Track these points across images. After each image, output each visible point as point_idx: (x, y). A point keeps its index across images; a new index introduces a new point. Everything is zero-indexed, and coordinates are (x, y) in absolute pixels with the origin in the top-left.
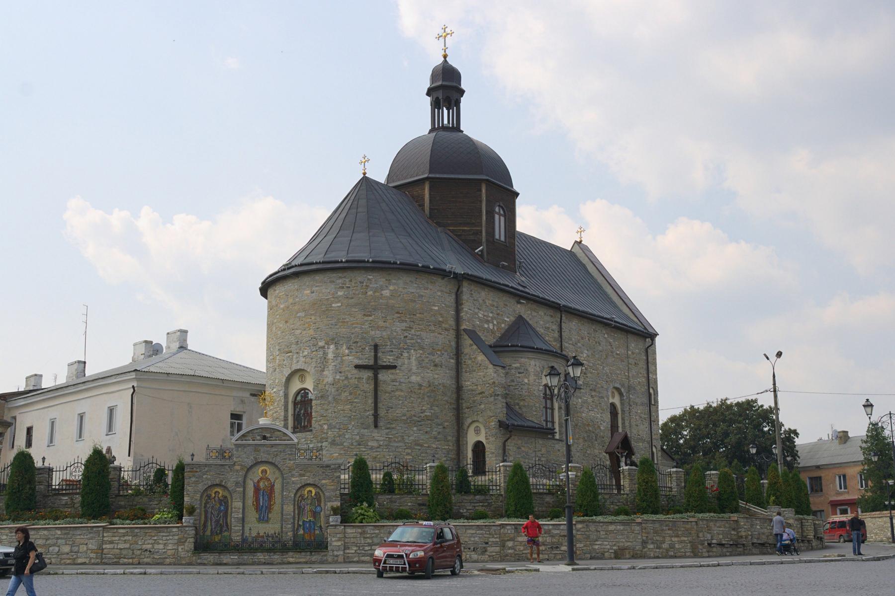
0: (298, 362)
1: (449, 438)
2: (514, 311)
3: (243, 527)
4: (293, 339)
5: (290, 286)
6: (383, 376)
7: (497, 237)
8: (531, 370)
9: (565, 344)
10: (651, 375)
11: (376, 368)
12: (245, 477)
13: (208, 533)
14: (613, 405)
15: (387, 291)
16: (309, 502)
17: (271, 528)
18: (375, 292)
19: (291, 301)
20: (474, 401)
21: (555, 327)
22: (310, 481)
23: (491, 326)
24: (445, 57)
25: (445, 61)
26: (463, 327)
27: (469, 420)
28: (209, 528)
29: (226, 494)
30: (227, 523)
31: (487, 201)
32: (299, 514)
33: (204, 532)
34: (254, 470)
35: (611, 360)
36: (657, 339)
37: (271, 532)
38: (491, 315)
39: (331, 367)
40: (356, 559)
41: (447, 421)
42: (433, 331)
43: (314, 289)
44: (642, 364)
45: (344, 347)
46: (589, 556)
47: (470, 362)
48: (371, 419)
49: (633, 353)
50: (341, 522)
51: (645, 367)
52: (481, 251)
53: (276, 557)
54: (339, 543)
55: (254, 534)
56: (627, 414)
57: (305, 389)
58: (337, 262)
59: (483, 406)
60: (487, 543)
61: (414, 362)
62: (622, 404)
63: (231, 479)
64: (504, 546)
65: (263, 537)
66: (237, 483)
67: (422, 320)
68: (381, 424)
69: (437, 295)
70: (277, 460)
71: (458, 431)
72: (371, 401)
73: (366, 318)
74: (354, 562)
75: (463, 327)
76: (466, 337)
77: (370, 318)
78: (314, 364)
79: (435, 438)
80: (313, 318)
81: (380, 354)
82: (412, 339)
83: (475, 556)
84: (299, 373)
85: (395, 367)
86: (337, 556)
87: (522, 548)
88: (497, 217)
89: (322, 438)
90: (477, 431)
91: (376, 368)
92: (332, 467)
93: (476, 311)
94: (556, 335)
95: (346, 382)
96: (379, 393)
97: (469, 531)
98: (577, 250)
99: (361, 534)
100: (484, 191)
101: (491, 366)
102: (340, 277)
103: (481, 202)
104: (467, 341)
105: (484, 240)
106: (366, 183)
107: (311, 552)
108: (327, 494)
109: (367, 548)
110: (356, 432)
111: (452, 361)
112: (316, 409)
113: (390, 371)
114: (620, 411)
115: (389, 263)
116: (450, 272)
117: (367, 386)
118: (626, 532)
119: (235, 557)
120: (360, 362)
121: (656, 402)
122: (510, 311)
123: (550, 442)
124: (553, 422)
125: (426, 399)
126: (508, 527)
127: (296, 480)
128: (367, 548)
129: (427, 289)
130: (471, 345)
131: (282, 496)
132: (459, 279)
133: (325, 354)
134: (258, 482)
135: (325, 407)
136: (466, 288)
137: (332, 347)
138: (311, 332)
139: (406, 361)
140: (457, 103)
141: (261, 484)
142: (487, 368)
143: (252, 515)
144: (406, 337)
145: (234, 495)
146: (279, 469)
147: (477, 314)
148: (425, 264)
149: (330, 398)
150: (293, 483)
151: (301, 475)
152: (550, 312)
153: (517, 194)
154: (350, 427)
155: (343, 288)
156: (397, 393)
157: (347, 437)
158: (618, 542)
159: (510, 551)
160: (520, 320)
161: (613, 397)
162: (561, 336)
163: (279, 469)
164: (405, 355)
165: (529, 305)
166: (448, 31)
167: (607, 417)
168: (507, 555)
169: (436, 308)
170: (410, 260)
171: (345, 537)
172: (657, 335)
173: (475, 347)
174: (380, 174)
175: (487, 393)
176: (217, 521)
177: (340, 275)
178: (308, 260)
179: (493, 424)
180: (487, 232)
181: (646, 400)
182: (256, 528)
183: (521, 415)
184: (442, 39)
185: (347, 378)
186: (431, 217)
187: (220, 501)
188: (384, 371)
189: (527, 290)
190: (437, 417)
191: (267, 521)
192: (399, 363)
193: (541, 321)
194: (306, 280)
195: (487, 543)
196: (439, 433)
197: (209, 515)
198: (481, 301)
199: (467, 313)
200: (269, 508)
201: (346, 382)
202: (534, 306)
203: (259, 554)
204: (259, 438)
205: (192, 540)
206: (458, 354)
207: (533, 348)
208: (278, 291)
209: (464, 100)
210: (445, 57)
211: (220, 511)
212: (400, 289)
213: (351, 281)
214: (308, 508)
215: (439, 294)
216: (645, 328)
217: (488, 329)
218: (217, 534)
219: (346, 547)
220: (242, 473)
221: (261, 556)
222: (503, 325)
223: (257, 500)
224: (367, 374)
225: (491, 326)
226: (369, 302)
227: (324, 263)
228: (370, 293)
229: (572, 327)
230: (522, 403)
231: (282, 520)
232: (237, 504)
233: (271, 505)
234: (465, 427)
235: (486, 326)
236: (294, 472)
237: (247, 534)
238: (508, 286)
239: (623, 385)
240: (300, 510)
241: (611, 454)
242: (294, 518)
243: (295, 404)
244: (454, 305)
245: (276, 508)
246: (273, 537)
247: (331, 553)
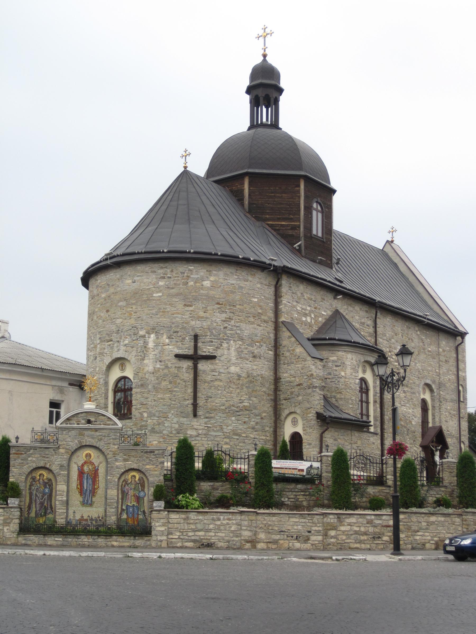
0: (118, 350)
1: (267, 429)
2: (331, 305)
3: (67, 509)
4: (114, 328)
5: (112, 275)
6: (203, 366)
7: (314, 232)
8: (348, 363)
9: (379, 340)
10: (460, 373)
11: (195, 358)
12: (70, 460)
13: (33, 515)
14: (424, 401)
15: (208, 282)
16: (133, 486)
17: (94, 512)
18: (196, 282)
19: (112, 290)
20: (292, 393)
21: (370, 322)
22: (135, 466)
23: (309, 320)
24: (265, 56)
25: (265, 60)
26: (282, 319)
27: (287, 412)
28: (34, 510)
29: (51, 476)
30: (51, 505)
31: (306, 197)
32: (122, 499)
33: (29, 513)
34: (79, 453)
36: (467, 338)
37: (95, 516)
38: (309, 308)
39: (151, 356)
40: (179, 544)
41: (265, 412)
42: (253, 323)
43: (136, 278)
44: (452, 362)
45: (165, 337)
46: (410, 546)
47: (288, 354)
48: (190, 408)
49: (444, 351)
50: (165, 508)
51: (455, 364)
52: (299, 246)
53: (100, 540)
54: (163, 529)
55: (78, 517)
56: (437, 411)
57: (125, 378)
58: (159, 252)
59: (300, 398)
60: (309, 532)
61: (233, 353)
62: (433, 400)
63: (56, 461)
64: (326, 535)
65: (86, 520)
66: (61, 466)
67: (241, 311)
68: (200, 413)
69: (257, 288)
70: (100, 444)
71: (275, 422)
72: (190, 390)
73: (187, 308)
74: (177, 547)
75: (282, 319)
76: (285, 329)
77: (191, 308)
78: (134, 353)
79: (253, 428)
80: (134, 307)
81: (200, 344)
82: (231, 330)
83: (297, 545)
84: (120, 361)
85: (214, 357)
86: (161, 541)
87: (344, 537)
88: (314, 213)
89: (142, 426)
90: (295, 422)
91: (195, 358)
92: (156, 452)
93: (295, 303)
94: (371, 330)
95: (166, 371)
96: (198, 383)
97: (292, 520)
98: (388, 250)
99: (184, 519)
100: (302, 186)
101: (309, 358)
102: (162, 268)
103: (299, 197)
104: (285, 334)
105: (302, 235)
106: (186, 175)
107: (135, 536)
108: (151, 479)
109: (190, 534)
110: (175, 420)
111: (270, 352)
112: (137, 397)
113: (209, 361)
114: (430, 407)
115: (210, 254)
116: (270, 265)
117: (187, 375)
118: (447, 524)
119: (59, 539)
120: (181, 352)
121: (465, 399)
122: (326, 306)
123: (365, 435)
124: (368, 416)
125: (245, 389)
126: (331, 516)
127: (120, 465)
128: (190, 534)
129: (247, 281)
130: (289, 337)
131: (106, 480)
132: (278, 273)
133: (146, 343)
134: (83, 465)
135: (146, 395)
136: (285, 282)
137: (152, 336)
138: (132, 321)
139: (226, 352)
140: (276, 101)
141: (86, 468)
142: (305, 360)
143: (76, 498)
144: (225, 328)
145: (59, 479)
146: (103, 453)
147: (295, 307)
148: (246, 256)
149: (150, 387)
150: (117, 467)
151: (125, 460)
152: (365, 308)
153: (333, 191)
154: (170, 415)
155: (164, 278)
156: (217, 383)
157: (166, 425)
158: (439, 533)
159: (332, 540)
160: (337, 313)
161: (424, 393)
162: (376, 332)
163: (103, 453)
164: (225, 345)
165: (346, 300)
166: (268, 31)
167: (418, 412)
168: (329, 544)
169: (256, 300)
170: (229, 252)
171: (169, 522)
172: (466, 333)
173: (293, 339)
174: (200, 168)
175: (305, 385)
176: (42, 504)
177: (162, 265)
178: (129, 250)
179: (312, 415)
180: (305, 228)
181: (455, 397)
182: (79, 512)
183: (338, 407)
184: (261, 39)
185: (167, 367)
186: (250, 212)
187: (45, 484)
188: (204, 361)
189: (343, 285)
190: (255, 408)
191: (91, 505)
192: (218, 353)
193: (357, 316)
194: (128, 270)
195: (309, 532)
196: (257, 423)
197: (34, 497)
198: (299, 295)
199: (285, 304)
200: (93, 492)
201: (166, 371)
202: (350, 302)
203: (83, 537)
204: (83, 421)
205: (17, 521)
206: (276, 346)
207: (351, 342)
208: (100, 280)
209: (283, 99)
210: (265, 56)
211: (44, 494)
212: (221, 280)
213: (172, 271)
214: (131, 493)
215: (259, 286)
216: (456, 327)
217: (306, 323)
218: (41, 516)
219: (169, 533)
220: (66, 456)
221: (85, 540)
222: (320, 319)
223: (81, 484)
224: (187, 364)
225: (309, 319)
226: (190, 293)
227: (145, 253)
228: (191, 283)
229: (386, 324)
230: (338, 396)
231: (106, 504)
232: (61, 487)
233: (95, 489)
234: (282, 418)
236: (118, 457)
237: (71, 516)
238: (325, 280)
239: (434, 382)
240: (124, 494)
241: (425, 448)
242: (118, 503)
243: (116, 391)
244: (273, 297)
245: (100, 492)
246: (96, 521)
247: (154, 538)
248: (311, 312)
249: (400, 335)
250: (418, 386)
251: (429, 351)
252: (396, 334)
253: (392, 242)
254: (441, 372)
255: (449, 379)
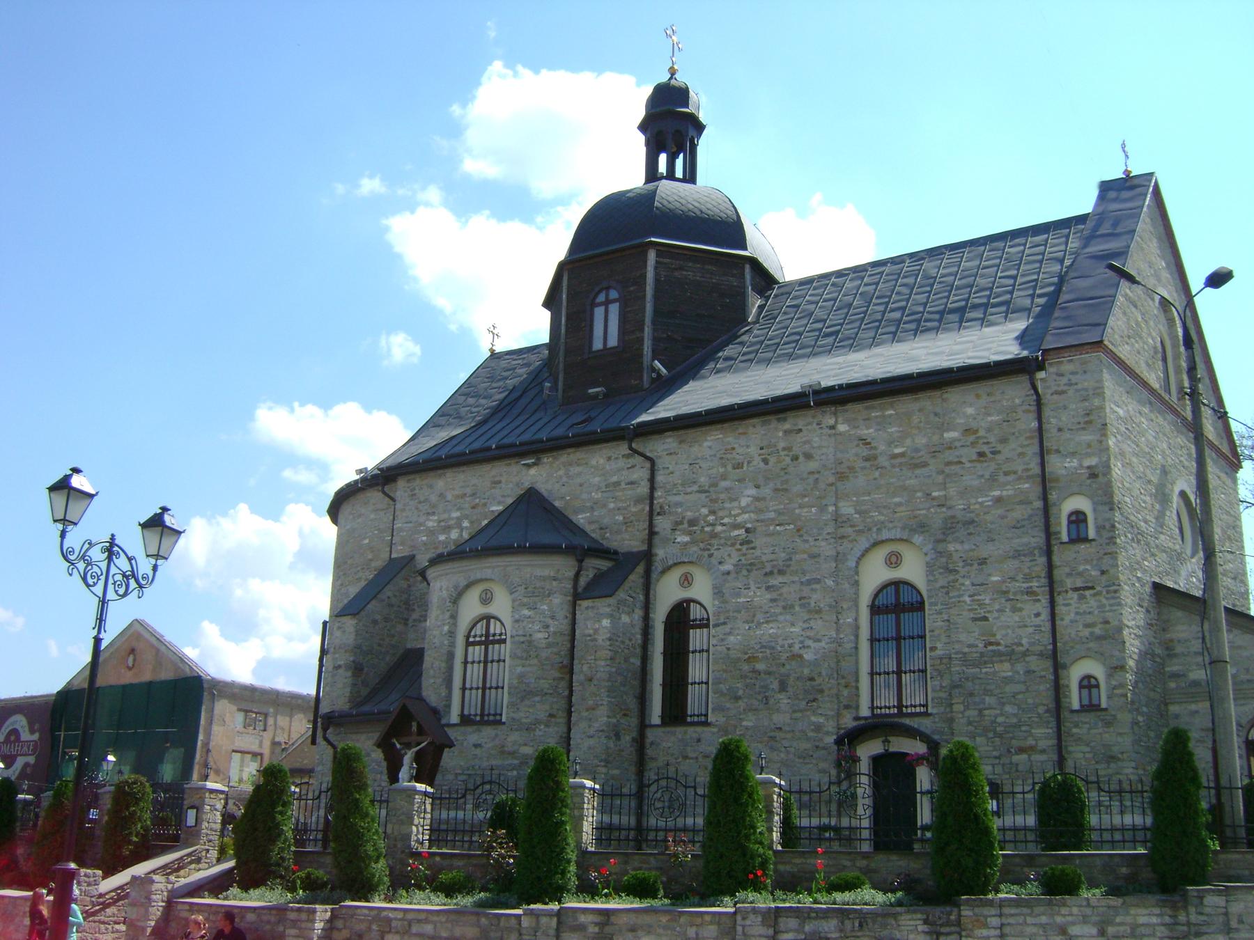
7: (598, 345)
21: (641, 474)
24: (673, 72)
35: (860, 481)
88: (599, 312)
94: (644, 489)
181: (1035, 538)
198: (433, 498)
225: (454, 535)
235: (442, 538)
248: (459, 519)
249: (757, 461)
250: (838, 558)
251: (895, 456)
252: (738, 466)
253: (1127, 172)
254: (952, 491)
255: (998, 500)
